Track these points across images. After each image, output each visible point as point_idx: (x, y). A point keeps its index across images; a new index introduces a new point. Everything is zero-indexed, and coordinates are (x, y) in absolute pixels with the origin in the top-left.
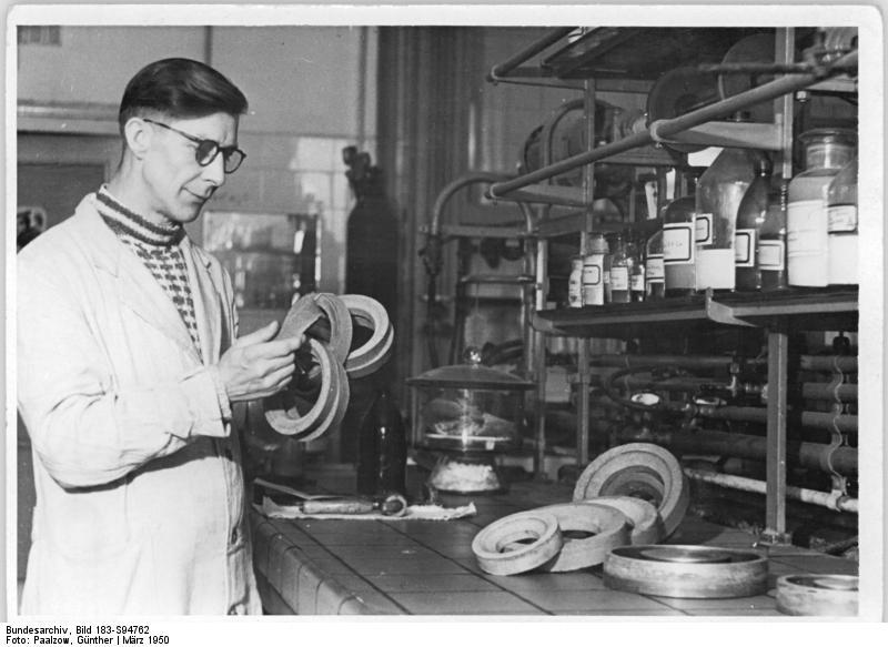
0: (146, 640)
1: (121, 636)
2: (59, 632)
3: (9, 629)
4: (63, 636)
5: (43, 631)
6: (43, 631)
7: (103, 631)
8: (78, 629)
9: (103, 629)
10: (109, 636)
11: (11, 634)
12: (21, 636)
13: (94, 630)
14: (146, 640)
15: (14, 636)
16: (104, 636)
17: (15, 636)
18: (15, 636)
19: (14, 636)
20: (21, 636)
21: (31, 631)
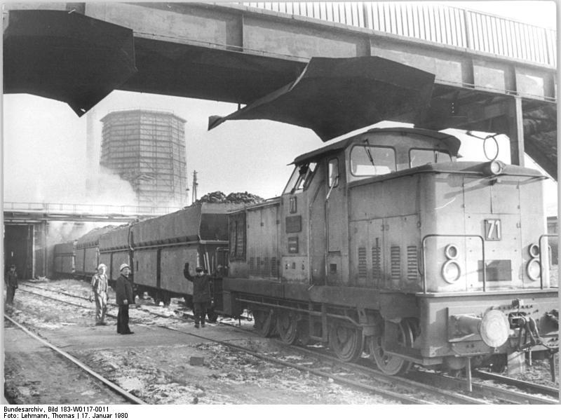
0: (114, 416)
1: (80, 413)
2: (38, 410)
3: (5, 409)
4: (40, 413)
5: (27, 410)
6: (27, 410)
7: (65, 409)
8: (50, 409)
9: (65, 409)
10: (72, 412)
11: (7, 412)
12: (13, 413)
13: (59, 409)
14: (114, 416)
15: (9, 413)
16: (67, 413)
17: (10, 413)
18: (10, 413)
19: (9, 413)
20: (13, 413)
21: (20, 410)
